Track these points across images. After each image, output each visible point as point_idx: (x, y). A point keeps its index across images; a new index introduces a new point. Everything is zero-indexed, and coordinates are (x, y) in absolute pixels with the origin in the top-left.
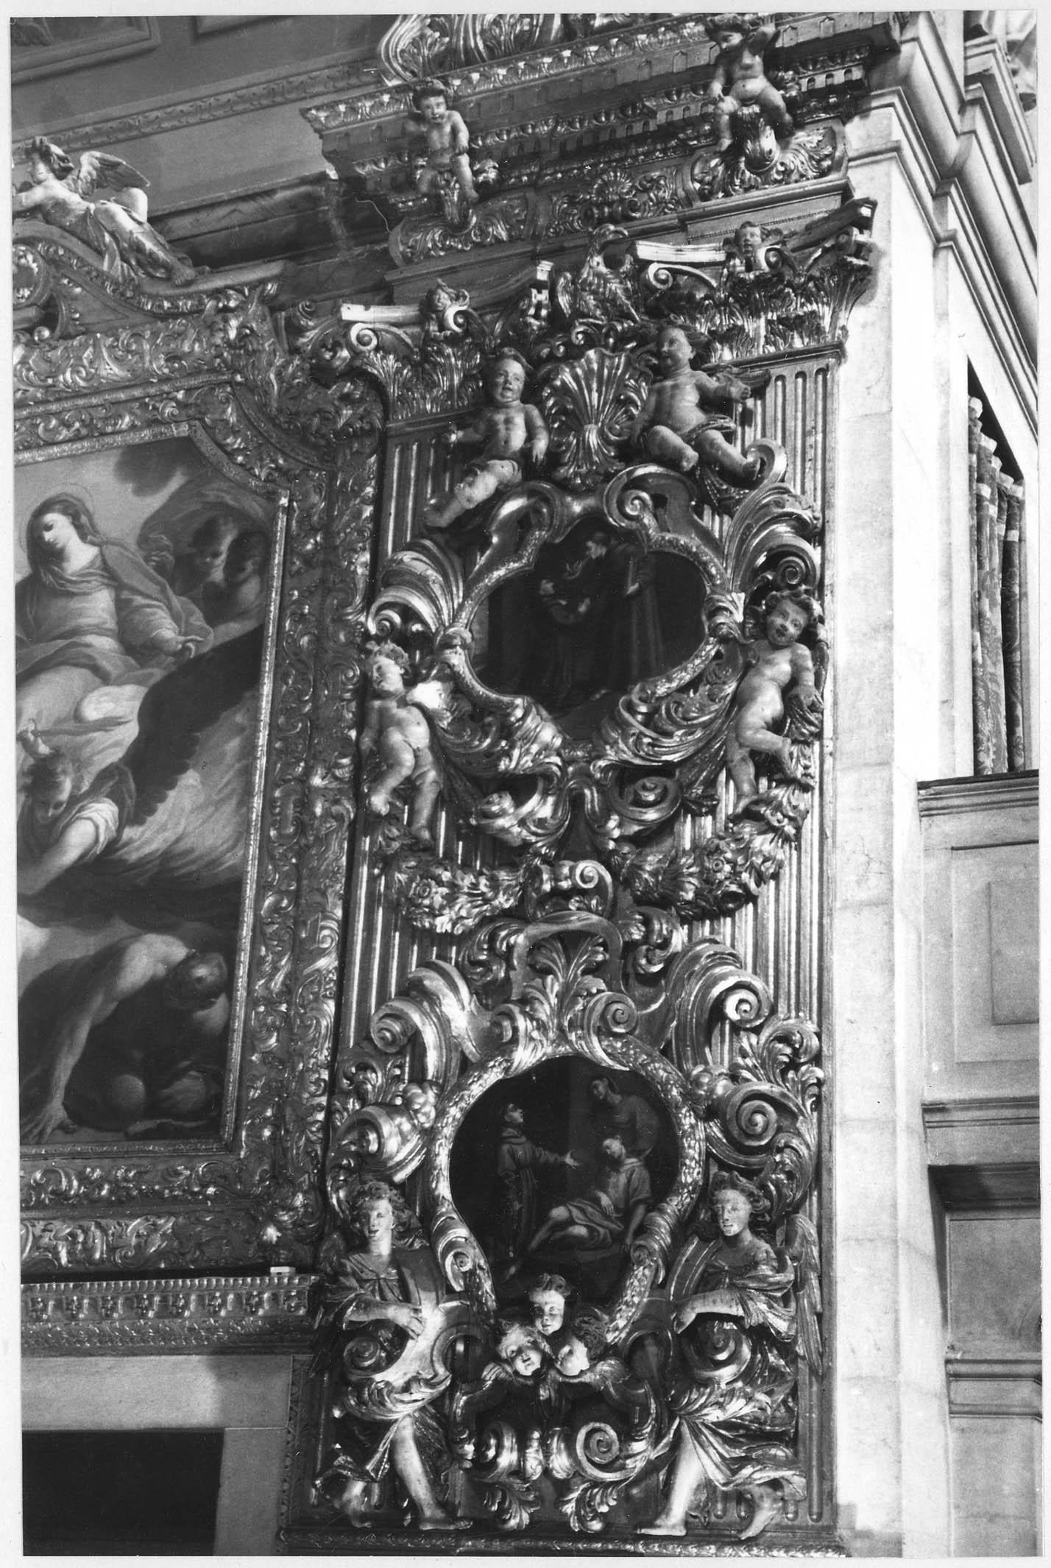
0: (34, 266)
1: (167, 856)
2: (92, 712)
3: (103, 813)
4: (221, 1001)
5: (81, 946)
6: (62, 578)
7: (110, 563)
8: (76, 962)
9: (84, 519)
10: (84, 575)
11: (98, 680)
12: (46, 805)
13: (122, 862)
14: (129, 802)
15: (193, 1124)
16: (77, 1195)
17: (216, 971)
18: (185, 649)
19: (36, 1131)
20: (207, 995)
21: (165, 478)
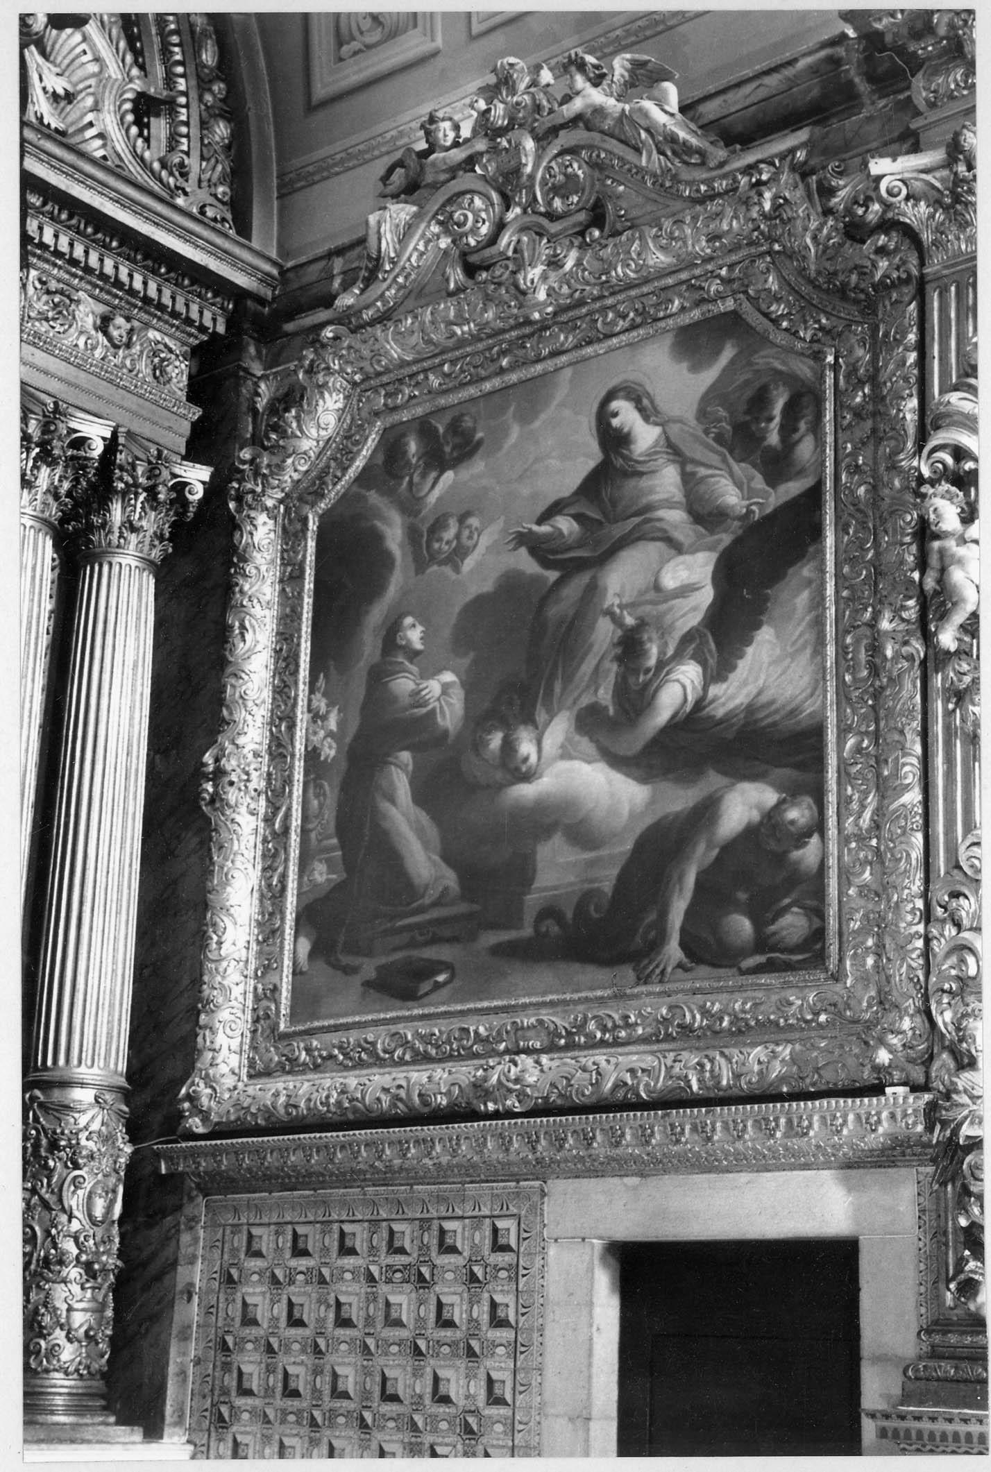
0: (580, 173)
1: (751, 709)
2: (670, 581)
3: (689, 674)
4: (815, 840)
5: (680, 799)
6: (631, 460)
7: (673, 439)
8: (677, 815)
9: (645, 402)
10: (651, 454)
11: (673, 552)
12: (636, 672)
13: (711, 717)
14: (712, 662)
15: (800, 957)
16: (700, 1027)
17: (807, 813)
18: (749, 512)
19: (658, 971)
21: (717, 353)
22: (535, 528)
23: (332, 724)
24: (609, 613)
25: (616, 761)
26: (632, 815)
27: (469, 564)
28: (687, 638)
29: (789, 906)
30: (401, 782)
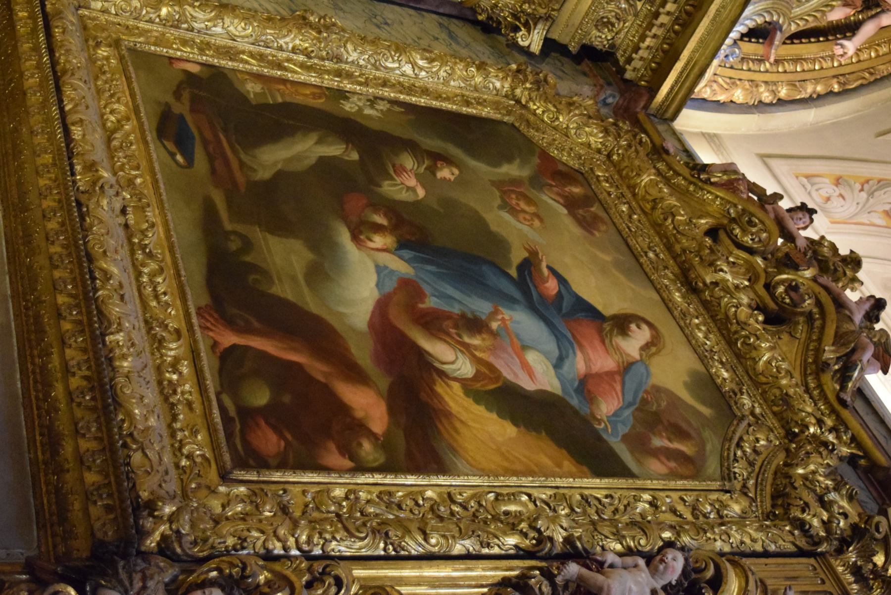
0: (806, 304)
1: (448, 415)
2: (532, 357)
6: (611, 335)
7: (634, 367)
8: (347, 349)
9: (654, 349)
10: (618, 349)
11: (554, 361)
12: (456, 327)
13: (434, 382)
14: (478, 386)
15: (239, 447)
16: (162, 356)
17: (371, 458)
18: (599, 421)
19: (209, 325)
20: (347, 451)
21: (704, 402)
22: (544, 265)
23: (368, 111)
24: (496, 312)
25: (382, 306)
26: (340, 315)
27: (507, 217)
28: (491, 367)
29: (285, 439)
30: (335, 150)
